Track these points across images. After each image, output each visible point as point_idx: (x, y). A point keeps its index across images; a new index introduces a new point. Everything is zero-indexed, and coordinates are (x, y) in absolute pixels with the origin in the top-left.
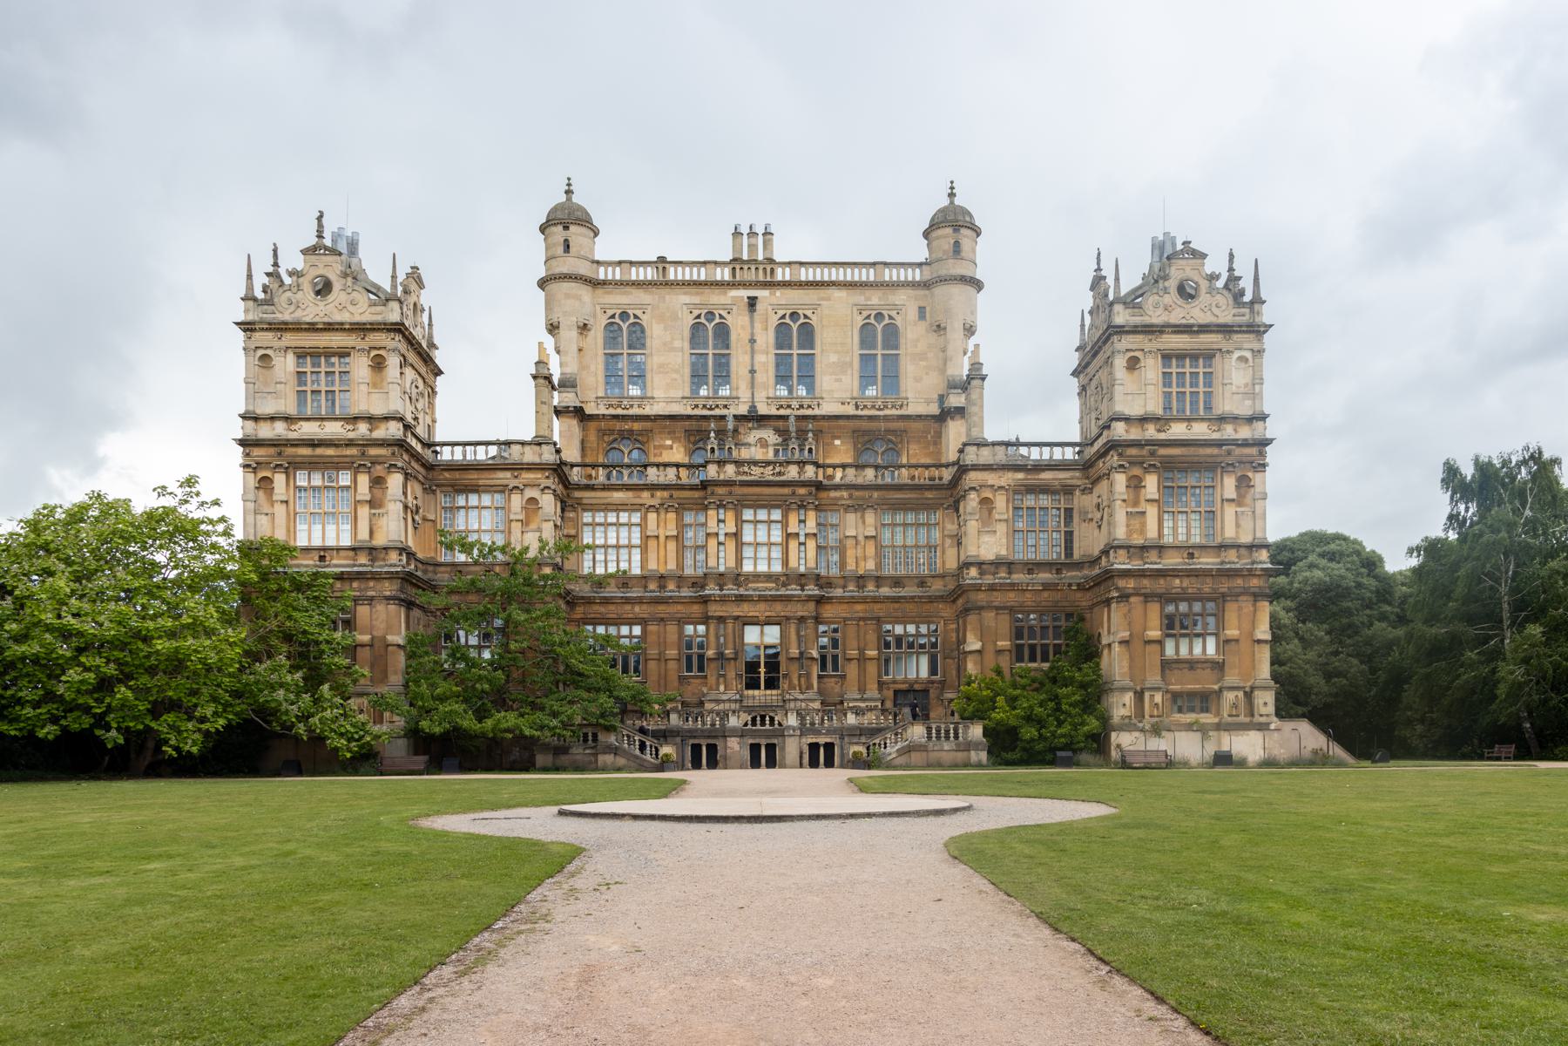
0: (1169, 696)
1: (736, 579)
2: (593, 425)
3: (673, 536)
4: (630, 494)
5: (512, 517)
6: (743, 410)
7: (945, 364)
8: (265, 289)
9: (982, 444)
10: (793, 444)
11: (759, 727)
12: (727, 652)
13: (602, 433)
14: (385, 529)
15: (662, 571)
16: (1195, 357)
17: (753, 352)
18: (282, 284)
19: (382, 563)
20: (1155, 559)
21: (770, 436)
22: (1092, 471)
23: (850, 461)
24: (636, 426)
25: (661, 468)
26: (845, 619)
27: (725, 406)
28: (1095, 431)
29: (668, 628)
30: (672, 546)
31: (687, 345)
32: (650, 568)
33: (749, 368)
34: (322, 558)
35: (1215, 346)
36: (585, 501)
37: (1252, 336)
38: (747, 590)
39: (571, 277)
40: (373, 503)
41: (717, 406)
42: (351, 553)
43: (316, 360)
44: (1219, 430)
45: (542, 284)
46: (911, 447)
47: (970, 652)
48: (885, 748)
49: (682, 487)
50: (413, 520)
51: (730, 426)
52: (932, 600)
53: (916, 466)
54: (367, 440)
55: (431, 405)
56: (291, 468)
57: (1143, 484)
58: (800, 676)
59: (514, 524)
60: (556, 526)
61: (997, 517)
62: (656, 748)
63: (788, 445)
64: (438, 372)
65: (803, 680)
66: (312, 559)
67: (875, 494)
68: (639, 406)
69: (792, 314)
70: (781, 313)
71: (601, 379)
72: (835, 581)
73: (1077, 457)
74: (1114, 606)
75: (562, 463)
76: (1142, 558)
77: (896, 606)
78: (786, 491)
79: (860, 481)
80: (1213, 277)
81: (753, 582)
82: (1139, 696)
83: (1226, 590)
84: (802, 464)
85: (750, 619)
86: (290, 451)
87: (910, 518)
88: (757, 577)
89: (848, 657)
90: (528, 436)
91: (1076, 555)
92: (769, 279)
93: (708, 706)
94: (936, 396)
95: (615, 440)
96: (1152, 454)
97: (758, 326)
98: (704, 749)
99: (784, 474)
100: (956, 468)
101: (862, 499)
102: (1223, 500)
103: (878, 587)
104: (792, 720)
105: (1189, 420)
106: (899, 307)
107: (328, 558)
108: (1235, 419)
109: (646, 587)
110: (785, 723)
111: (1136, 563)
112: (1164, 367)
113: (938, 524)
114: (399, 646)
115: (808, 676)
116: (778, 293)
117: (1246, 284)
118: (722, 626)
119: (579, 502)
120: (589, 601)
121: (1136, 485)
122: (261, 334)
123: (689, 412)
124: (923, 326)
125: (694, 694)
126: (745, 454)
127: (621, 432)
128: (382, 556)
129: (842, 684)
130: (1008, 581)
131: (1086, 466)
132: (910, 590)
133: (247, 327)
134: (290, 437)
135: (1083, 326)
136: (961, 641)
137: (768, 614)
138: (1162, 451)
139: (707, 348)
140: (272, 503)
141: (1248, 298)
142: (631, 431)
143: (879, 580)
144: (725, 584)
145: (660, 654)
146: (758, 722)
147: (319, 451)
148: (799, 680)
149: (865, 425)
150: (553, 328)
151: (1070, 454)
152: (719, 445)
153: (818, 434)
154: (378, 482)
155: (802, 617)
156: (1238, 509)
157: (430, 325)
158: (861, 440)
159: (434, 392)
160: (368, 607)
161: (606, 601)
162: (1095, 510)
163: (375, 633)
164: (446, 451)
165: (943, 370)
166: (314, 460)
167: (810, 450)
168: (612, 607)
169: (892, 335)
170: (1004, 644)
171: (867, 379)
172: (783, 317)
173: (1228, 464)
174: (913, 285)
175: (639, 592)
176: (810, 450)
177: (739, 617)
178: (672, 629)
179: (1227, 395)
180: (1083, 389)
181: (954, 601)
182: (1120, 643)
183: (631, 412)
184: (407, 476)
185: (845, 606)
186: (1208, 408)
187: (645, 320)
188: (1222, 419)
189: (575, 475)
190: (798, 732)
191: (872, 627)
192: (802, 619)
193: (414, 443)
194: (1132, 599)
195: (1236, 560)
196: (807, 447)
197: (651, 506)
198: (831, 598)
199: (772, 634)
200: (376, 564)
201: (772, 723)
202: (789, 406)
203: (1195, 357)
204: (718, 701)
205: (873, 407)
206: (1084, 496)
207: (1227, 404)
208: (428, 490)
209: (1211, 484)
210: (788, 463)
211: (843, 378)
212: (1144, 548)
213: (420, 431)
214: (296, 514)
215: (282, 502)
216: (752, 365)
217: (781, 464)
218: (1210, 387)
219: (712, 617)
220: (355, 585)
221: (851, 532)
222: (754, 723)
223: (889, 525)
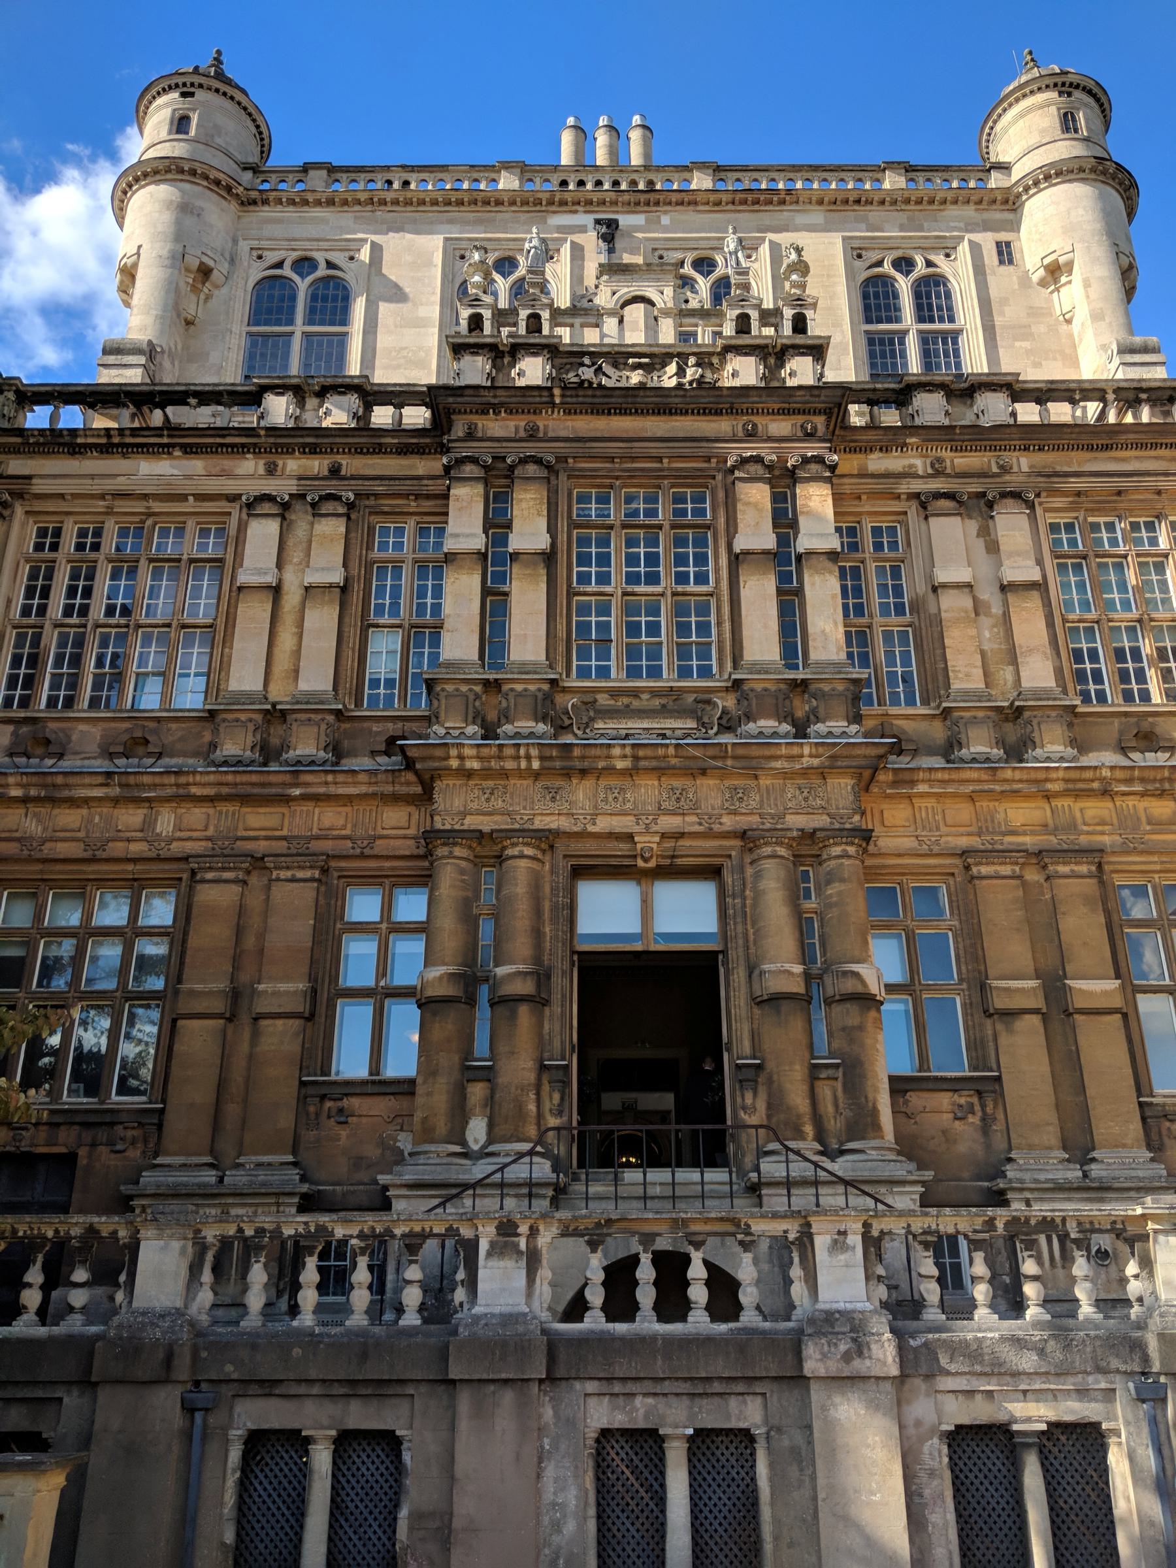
1: (548, 698)
3: (331, 586)
4: (197, 465)
11: (647, 1323)
12: (501, 971)
15: (279, 693)
29: (280, 892)
32: (234, 685)
65: (825, 1091)
89: (1000, 1002)
98: (322, 1458)
103: (1082, 746)
146: (646, 1296)
155: (809, 836)
168: (69, 818)
191: (1075, 885)
219: (451, 837)
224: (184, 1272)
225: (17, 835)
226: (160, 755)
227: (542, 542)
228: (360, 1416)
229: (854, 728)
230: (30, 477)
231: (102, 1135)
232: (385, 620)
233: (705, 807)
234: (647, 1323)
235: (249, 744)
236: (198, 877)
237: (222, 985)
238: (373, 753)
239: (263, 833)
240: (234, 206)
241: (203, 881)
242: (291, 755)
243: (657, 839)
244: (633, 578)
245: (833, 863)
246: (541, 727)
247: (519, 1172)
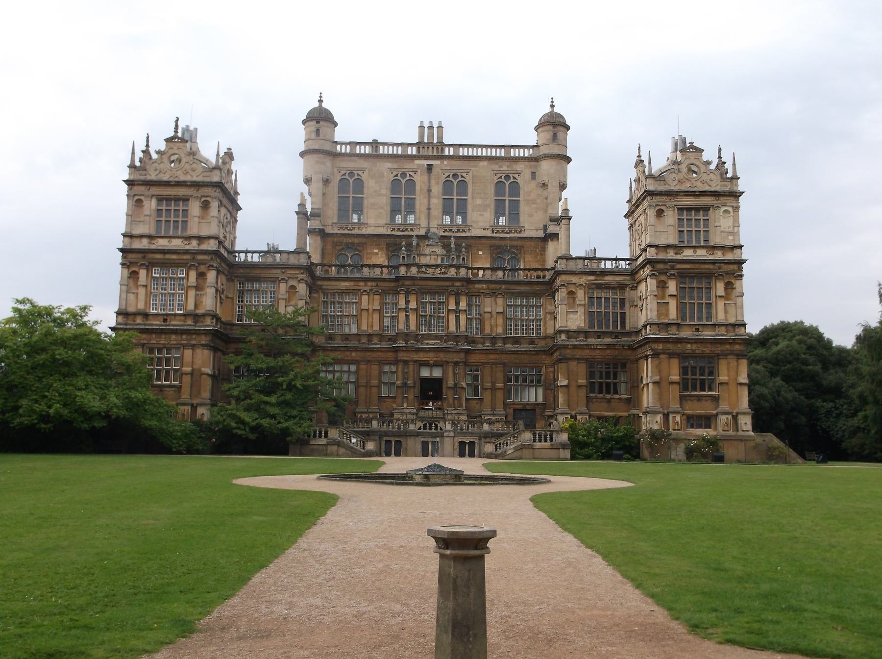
0: (685, 417)
1: (416, 337)
2: (329, 239)
4: (352, 283)
5: (280, 297)
6: (422, 232)
7: (547, 207)
8: (141, 160)
9: (569, 258)
10: (453, 255)
11: (428, 431)
13: (335, 244)
14: (204, 303)
15: (370, 331)
16: (697, 210)
17: (429, 197)
18: (151, 158)
19: (201, 324)
20: (675, 332)
21: (439, 251)
22: (637, 276)
23: (488, 265)
24: (357, 241)
25: (372, 268)
26: (483, 364)
27: (412, 230)
28: (638, 252)
30: (376, 316)
31: (389, 192)
33: (427, 207)
34: (165, 320)
35: (710, 204)
36: (324, 287)
37: (732, 199)
38: (422, 344)
39: (320, 151)
40: (198, 288)
41: (407, 229)
42: (183, 318)
43: (169, 202)
44: (713, 254)
45: (302, 154)
46: (526, 256)
47: (561, 386)
48: (507, 446)
49: (384, 280)
50: (220, 297)
51: (415, 243)
52: (537, 353)
53: (529, 270)
54: (196, 250)
55: (234, 228)
56: (150, 266)
57: (667, 286)
58: (454, 398)
59: (281, 301)
60: (306, 302)
61: (578, 302)
62: (363, 442)
63: (449, 256)
64: (240, 209)
66: (159, 320)
67: (503, 287)
68: (359, 229)
69: (453, 175)
70: (447, 174)
71: (336, 212)
73: (627, 266)
74: (650, 360)
75: (312, 264)
76: (667, 331)
77: (516, 356)
78: (447, 283)
79: (494, 278)
80: (708, 163)
81: (426, 339)
82: (666, 416)
83: (719, 352)
84: (458, 267)
85: (423, 363)
86: (151, 256)
87: (525, 302)
88: (429, 337)
89: (485, 387)
90: (292, 247)
91: (627, 328)
92: (440, 154)
93: (396, 416)
94: (542, 226)
95: (343, 249)
96: (673, 268)
97: (433, 182)
98: (393, 443)
99: (447, 273)
100: (553, 271)
101: (494, 289)
102: (716, 297)
103: (504, 344)
104: (449, 427)
105: (694, 247)
106: (520, 172)
107: (169, 320)
108: (723, 248)
109: (359, 341)
110: (444, 428)
111: (663, 334)
112: (679, 215)
113: (542, 305)
114: (208, 374)
115: (459, 399)
116: (445, 162)
117: (728, 166)
119: (320, 287)
120: (325, 349)
121: (662, 286)
122: (137, 187)
123: (389, 233)
124: (533, 184)
126: (424, 260)
127: (347, 244)
128: (201, 319)
129: (481, 405)
130: (585, 343)
131: (633, 273)
132: (525, 347)
133: (130, 183)
134: (151, 248)
135: (631, 188)
136: (555, 379)
137: (435, 359)
138: (679, 266)
139: (401, 194)
140: (137, 287)
141: (729, 175)
142: (353, 244)
143: (505, 340)
145: (367, 383)
146: (428, 428)
147: (167, 256)
148: (454, 402)
149: (498, 243)
150: (307, 181)
151: (623, 265)
152: (407, 255)
153: (468, 247)
154: (201, 275)
155: (457, 362)
156: (727, 302)
157: (236, 180)
158: (495, 251)
159: (236, 221)
160: (191, 350)
161: (335, 349)
162: (639, 300)
163: (195, 367)
164: (242, 256)
165: (546, 211)
166: (164, 261)
167: (463, 259)
169: (515, 188)
170: (582, 381)
171: (499, 213)
172: (448, 176)
173: (719, 275)
174: (529, 159)
175: (354, 344)
176: (463, 259)
177: (417, 360)
178: (375, 368)
179: (718, 233)
180: (631, 226)
181: (552, 354)
182: (654, 383)
183: (353, 232)
184: (219, 272)
185: (484, 356)
186: (706, 241)
187: (364, 177)
188: (715, 247)
189: (318, 271)
190: (452, 434)
192: (456, 364)
193: (223, 251)
194: (662, 356)
195: (726, 333)
196: (462, 257)
197: (364, 291)
198: (475, 350)
199: (437, 373)
200: (198, 324)
201: (436, 428)
202: (451, 230)
203: (697, 210)
204: (402, 413)
205: (503, 232)
206: (632, 291)
207: (715, 239)
208: (230, 279)
209: (708, 286)
210: (450, 266)
211: (485, 214)
212: (668, 325)
213: (227, 244)
214: (151, 293)
215: (143, 286)
216: (429, 204)
217: (445, 267)
218: (708, 227)
219: (400, 361)
220: (184, 337)
221: (488, 309)
222: (425, 428)
223: (512, 305)
227: (415, 307)
230: (322, 285)
232: (387, 315)
240: (332, 157)
242: (373, 342)
244: (431, 312)
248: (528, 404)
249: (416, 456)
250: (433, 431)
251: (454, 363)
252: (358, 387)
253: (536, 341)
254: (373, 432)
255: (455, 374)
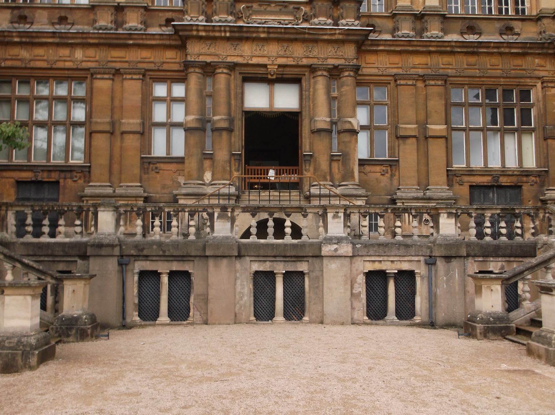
11: (271, 240)
12: (216, 118)
58: (332, 159)
72: (378, 22)
77: (472, 59)
89: (402, 133)
98: (165, 279)
103: (445, 31)
118: (209, 81)
125: (164, 187)
129: (392, 176)
144: (215, 13)
145: (113, 124)
146: (271, 231)
155: (336, 67)
185: (396, 59)
198: (377, 43)
224: (114, 222)
225: (19, 57)
226: (73, 24)
228: (176, 266)
229: (357, 22)
231: (68, 175)
233: (296, 55)
234: (271, 240)
235: (110, 21)
236: (94, 77)
237: (108, 120)
238: (160, 26)
239: (118, 59)
241: (96, 79)
242: (127, 26)
243: (276, 67)
245: (345, 79)
246: (230, 18)
247: (225, 191)
248: (504, 172)
249: (236, 321)
250: (288, 239)
251: (329, 70)
252: (90, 135)
253: (517, 26)
254: (100, 246)
255: (331, 99)
